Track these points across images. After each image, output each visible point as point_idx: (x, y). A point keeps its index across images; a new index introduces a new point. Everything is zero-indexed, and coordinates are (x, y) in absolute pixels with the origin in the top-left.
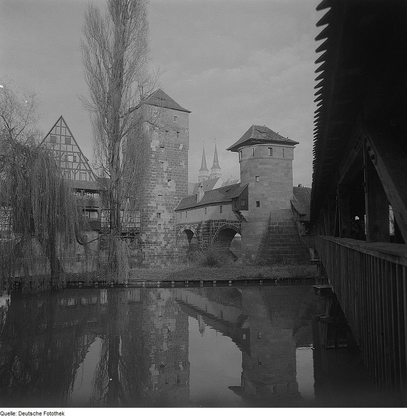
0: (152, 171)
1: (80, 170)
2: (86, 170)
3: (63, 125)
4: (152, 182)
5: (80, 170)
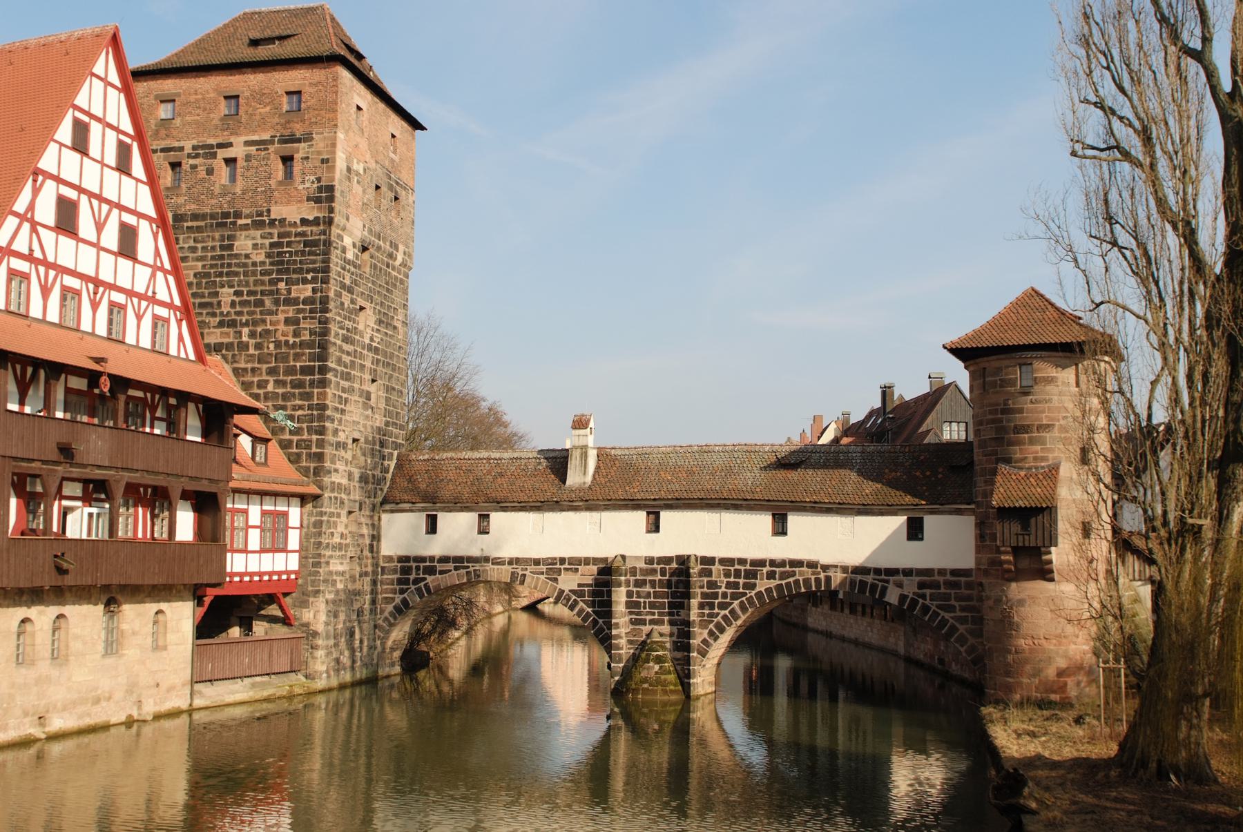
0: (346, 340)
1: (153, 300)
2: (170, 306)
3: (114, 77)
4: (342, 382)
5: (153, 300)
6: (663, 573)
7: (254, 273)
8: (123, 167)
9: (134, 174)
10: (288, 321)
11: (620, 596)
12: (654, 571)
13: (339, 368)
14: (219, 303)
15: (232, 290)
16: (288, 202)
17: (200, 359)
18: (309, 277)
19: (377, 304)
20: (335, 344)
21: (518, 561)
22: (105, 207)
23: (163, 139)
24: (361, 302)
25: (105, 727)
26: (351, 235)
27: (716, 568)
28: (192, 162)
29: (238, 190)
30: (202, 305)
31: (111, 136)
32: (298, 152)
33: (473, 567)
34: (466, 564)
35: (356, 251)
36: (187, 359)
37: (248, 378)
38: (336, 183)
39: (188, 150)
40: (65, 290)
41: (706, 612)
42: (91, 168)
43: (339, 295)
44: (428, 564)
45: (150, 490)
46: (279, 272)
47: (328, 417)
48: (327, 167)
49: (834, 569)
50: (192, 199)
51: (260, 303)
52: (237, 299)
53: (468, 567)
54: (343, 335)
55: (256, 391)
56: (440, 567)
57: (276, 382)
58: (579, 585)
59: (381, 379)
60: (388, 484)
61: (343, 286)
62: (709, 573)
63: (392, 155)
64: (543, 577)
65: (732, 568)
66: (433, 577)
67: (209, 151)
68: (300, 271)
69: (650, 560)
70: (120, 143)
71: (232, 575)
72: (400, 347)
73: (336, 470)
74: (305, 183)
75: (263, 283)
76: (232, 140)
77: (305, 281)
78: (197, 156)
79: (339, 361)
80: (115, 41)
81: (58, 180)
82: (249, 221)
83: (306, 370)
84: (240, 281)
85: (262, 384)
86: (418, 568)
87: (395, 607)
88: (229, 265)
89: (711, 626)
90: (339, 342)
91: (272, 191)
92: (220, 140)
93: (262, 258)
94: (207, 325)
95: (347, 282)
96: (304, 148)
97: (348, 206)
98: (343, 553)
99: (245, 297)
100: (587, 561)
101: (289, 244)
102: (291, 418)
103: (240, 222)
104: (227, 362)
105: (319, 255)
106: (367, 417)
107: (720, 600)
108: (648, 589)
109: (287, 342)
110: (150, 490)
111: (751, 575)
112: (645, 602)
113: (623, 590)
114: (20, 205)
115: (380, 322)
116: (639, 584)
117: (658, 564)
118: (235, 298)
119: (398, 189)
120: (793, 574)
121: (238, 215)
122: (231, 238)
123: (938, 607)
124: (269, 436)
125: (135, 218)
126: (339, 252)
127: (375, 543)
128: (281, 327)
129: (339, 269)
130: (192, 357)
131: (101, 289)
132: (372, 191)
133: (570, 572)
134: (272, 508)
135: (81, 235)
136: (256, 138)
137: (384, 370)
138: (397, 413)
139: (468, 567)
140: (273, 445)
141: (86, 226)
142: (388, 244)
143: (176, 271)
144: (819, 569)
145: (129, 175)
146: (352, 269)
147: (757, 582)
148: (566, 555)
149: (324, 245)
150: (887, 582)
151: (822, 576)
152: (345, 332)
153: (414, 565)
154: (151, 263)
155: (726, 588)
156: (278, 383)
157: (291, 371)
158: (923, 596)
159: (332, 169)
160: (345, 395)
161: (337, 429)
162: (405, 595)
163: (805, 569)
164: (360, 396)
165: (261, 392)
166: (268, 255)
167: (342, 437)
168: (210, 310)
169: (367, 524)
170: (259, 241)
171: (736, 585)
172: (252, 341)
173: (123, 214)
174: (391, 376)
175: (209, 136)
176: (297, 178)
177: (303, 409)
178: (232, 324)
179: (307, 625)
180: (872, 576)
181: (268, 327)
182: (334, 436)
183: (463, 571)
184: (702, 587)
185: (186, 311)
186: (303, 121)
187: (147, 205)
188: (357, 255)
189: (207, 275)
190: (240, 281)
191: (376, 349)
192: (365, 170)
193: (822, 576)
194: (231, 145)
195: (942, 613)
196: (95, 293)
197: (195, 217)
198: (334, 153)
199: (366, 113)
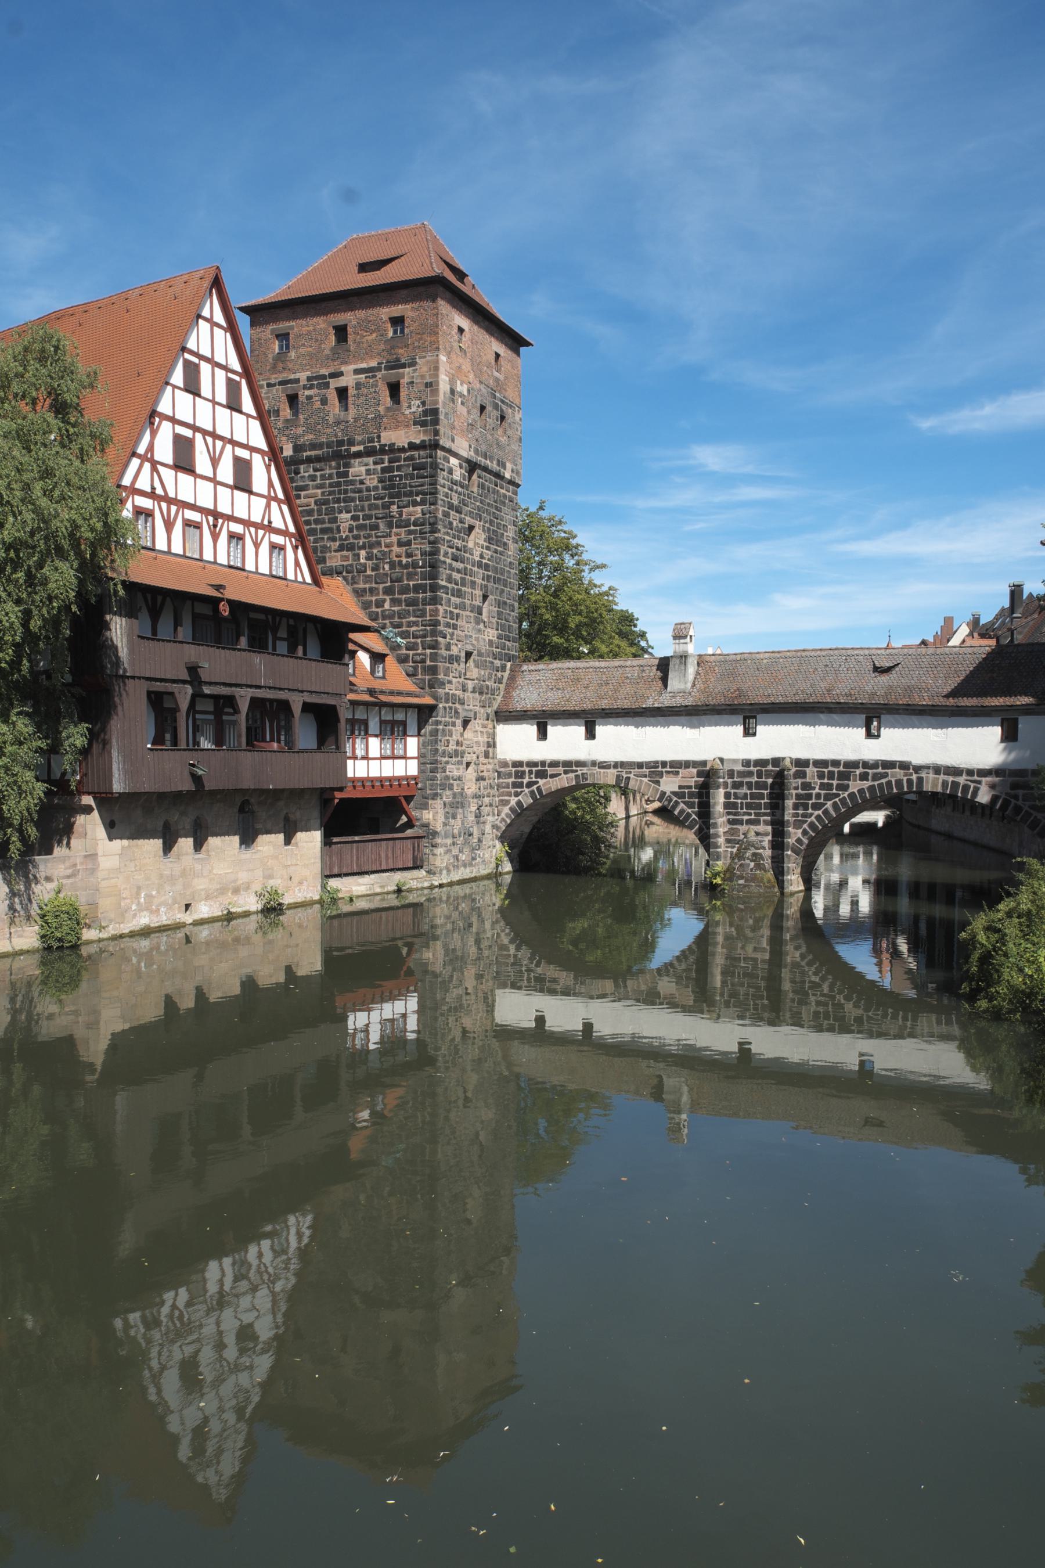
0: (455, 559)
1: (269, 528)
2: (284, 533)
3: (219, 317)
4: (453, 598)
5: (269, 528)
6: (759, 775)
7: (368, 498)
8: (234, 405)
9: (244, 410)
10: (400, 544)
11: (719, 797)
12: (750, 774)
13: (449, 585)
14: (338, 527)
15: (349, 515)
16: (397, 428)
17: (316, 582)
18: (418, 499)
19: (486, 522)
20: (445, 562)
21: (622, 765)
22: (219, 444)
23: (280, 372)
24: (469, 520)
25: (246, 914)
26: (456, 455)
27: (811, 771)
28: (307, 393)
29: (351, 419)
30: (324, 531)
31: (220, 374)
32: (403, 378)
33: (581, 771)
34: (574, 768)
35: (463, 471)
36: (304, 582)
37: (368, 598)
38: (440, 406)
39: (303, 381)
40: (188, 524)
41: (800, 812)
42: (204, 407)
43: (446, 515)
44: (540, 768)
45: (275, 704)
46: (391, 496)
47: (441, 632)
48: (431, 390)
49: (926, 771)
50: (310, 429)
51: (375, 527)
52: (354, 524)
53: (577, 771)
54: (453, 554)
55: (374, 609)
56: (550, 771)
57: (392, 600)
58: (680, 787)
59: (492, 594)
60: (502, 693)
61: (451, 506)
62: (803, 775)
63: (496, 374)
64: (645, 780)
65: (826, 770)
66: (544, 780)
67: (320, 381)
68: (410, 494)
69: (747, 763)
70: (229, 381)
71: (354, 780)
72: (510, 563)
73: (450, 682)
74: (412, 408)
75: (376, 507)
76: (343, 369)
77: (415, 504)
78: (311, 387)
79: (449, 579)
80: (217, 283)
81: (173, 420)
82: (361, 448)
83: (417, 588)
84: (356, 506)
85: (380, 604)
86: (531, 772)
87: (511, 809)
88: (346, 492)
89: (805, 826)
90: (448, 561)
91: (381, 417)
92: (332, 370)
93: (375, 483)
94: (328, 549)
95: (455, 502)
96: (409, 373)
97: (453, 428)
98: (459, 759)
99: (361, 522)
100: (687, 764)
101: (399, 468)
102: (404, 635)
103: (354, 449)
104: (348, 583)
105: (426, 477)
106: (479, 630)
107: (814, 801)
108: (744, 790)
109: (400, 562)
110: (275, 704)
111: (844, 776)
112: (742, 803)
113: (721, 791)
114: (141, 450)
115: (489, 540)
116: (737, 785)
117: (755, 766)
118: (352, 522)
119: (504, 407)
120: (886, 775)
121: (352, 443)
122: (348, 465)
123: (1032, 807)
124: (387, 651)
125: (248, 452)
126: (445, 473)
127: (491, 750)
128: (395, 549)
129: (446, 490)
130: (308, 580)
131: (220, 521)
132: (476, 412)
133: (671, 775)
134: (389, 718)
135: (199, 470)
136: (364, 365)
137: (495, 586)
138: (509, 626)
139: (577, 771)
140: (390, 661)
141: (202, 464)
142: (495, 462)
143: (289, 500)
144: (911, 771)
145: (240, 412)
146: (460, 489)
147: (850, 783)
148: (668, 757)
149: (431, 468)
150: (979, 782)
151: (914, 777)
152: (454, 550)
153: (527, 769)
154: (266, 493)
155: (820, 789)
156: (394, 602)
157: (405, 590)
158: (1016, 797)
159: (435, 392)
160: (456, 611)
161: (449, 643)
162: (520, 797)
163: (897, 770)
164: (471, 611)
165: (379, 610)
166: (381, 481)
167: (455, 650)
168: (330, 535)
169: (481, 732)
170: (372, 467)
171: (829, 787)
172: (369, 563)
173: (237, 449)
174: (502, 591)
175: (322, 367)
176: (404, 404)
177: (417, 626)
178: (351, 548)
179: (427, 825)
180: (964, 777)
181: (383, 548)
182: (446, 650)
183: (572, 775)
184: (796, 788)
185: (301, 539)
186: (407, 346)
187: (258, 440)
188: (464, 475)
189: (326, 502)
190: (356, 506)
191: (487, 565)
192: (469, 391)
193: (914, 777)
194: (341, 374)
195: (1035, 813)
196: (215, 526)
197: (314, 446)
198: (437, 376)
199: (467, 335)
